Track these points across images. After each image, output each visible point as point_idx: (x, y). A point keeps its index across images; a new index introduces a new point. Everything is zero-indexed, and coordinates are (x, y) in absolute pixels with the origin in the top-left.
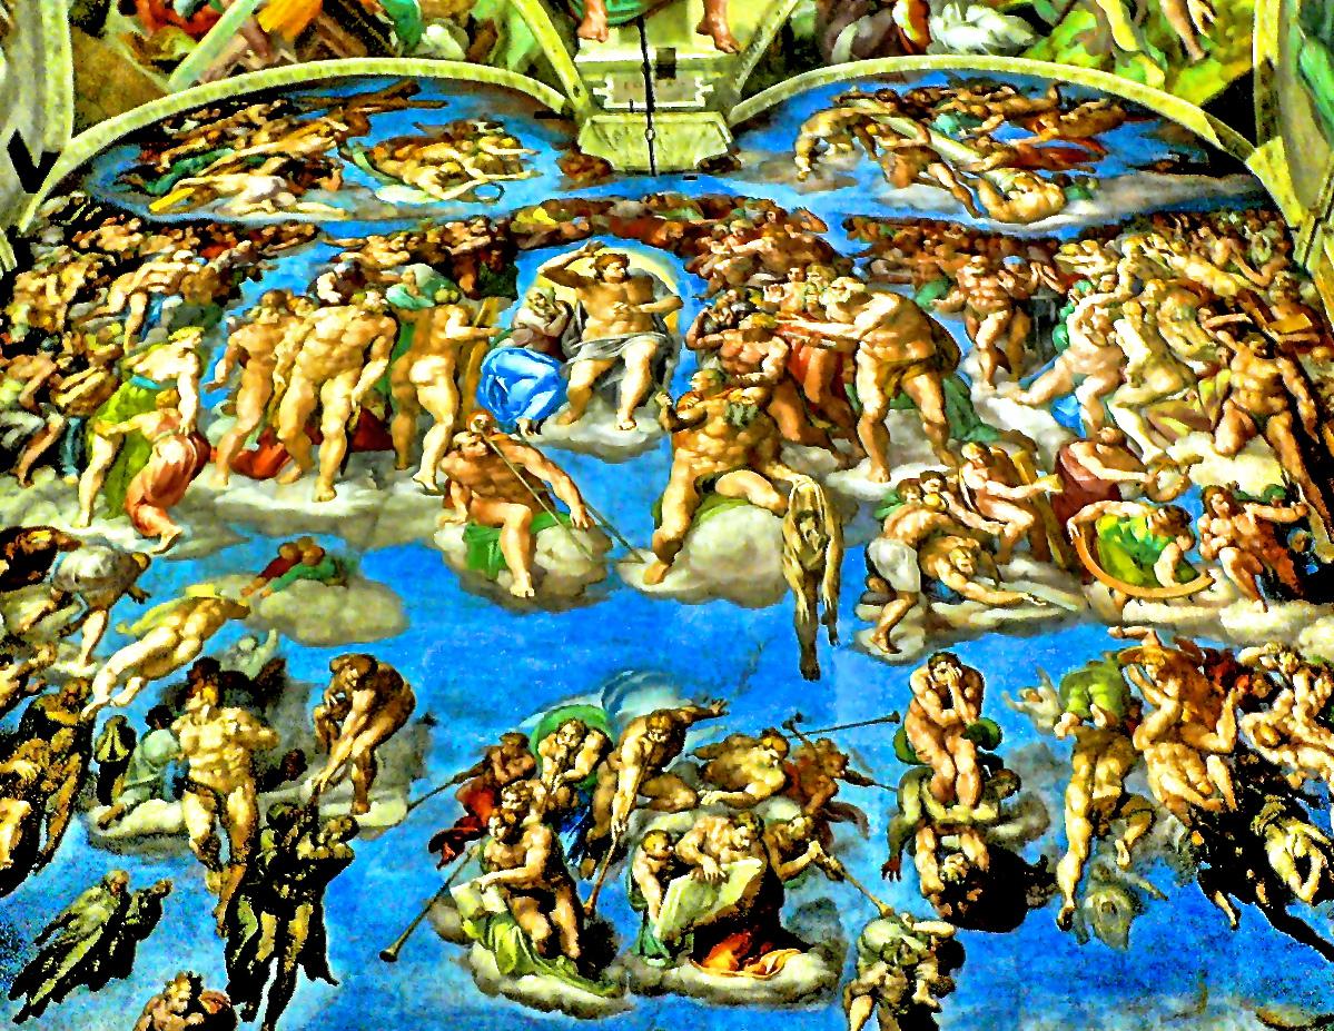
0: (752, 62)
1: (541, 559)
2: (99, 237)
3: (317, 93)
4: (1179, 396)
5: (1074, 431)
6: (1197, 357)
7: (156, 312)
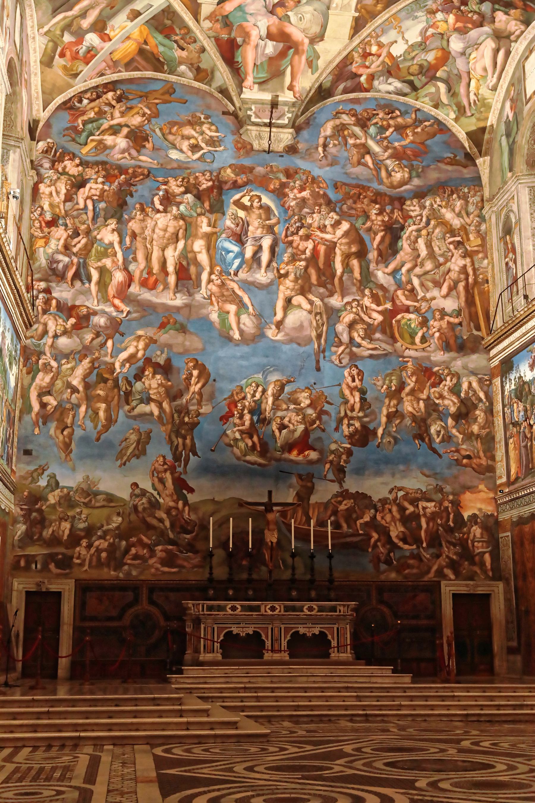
0: (306, 102)
1: (242, 326)
3: (133, 87)
4: (433, 273)
5: (399, 285)
6: (442, 255)
7: (98, 210)
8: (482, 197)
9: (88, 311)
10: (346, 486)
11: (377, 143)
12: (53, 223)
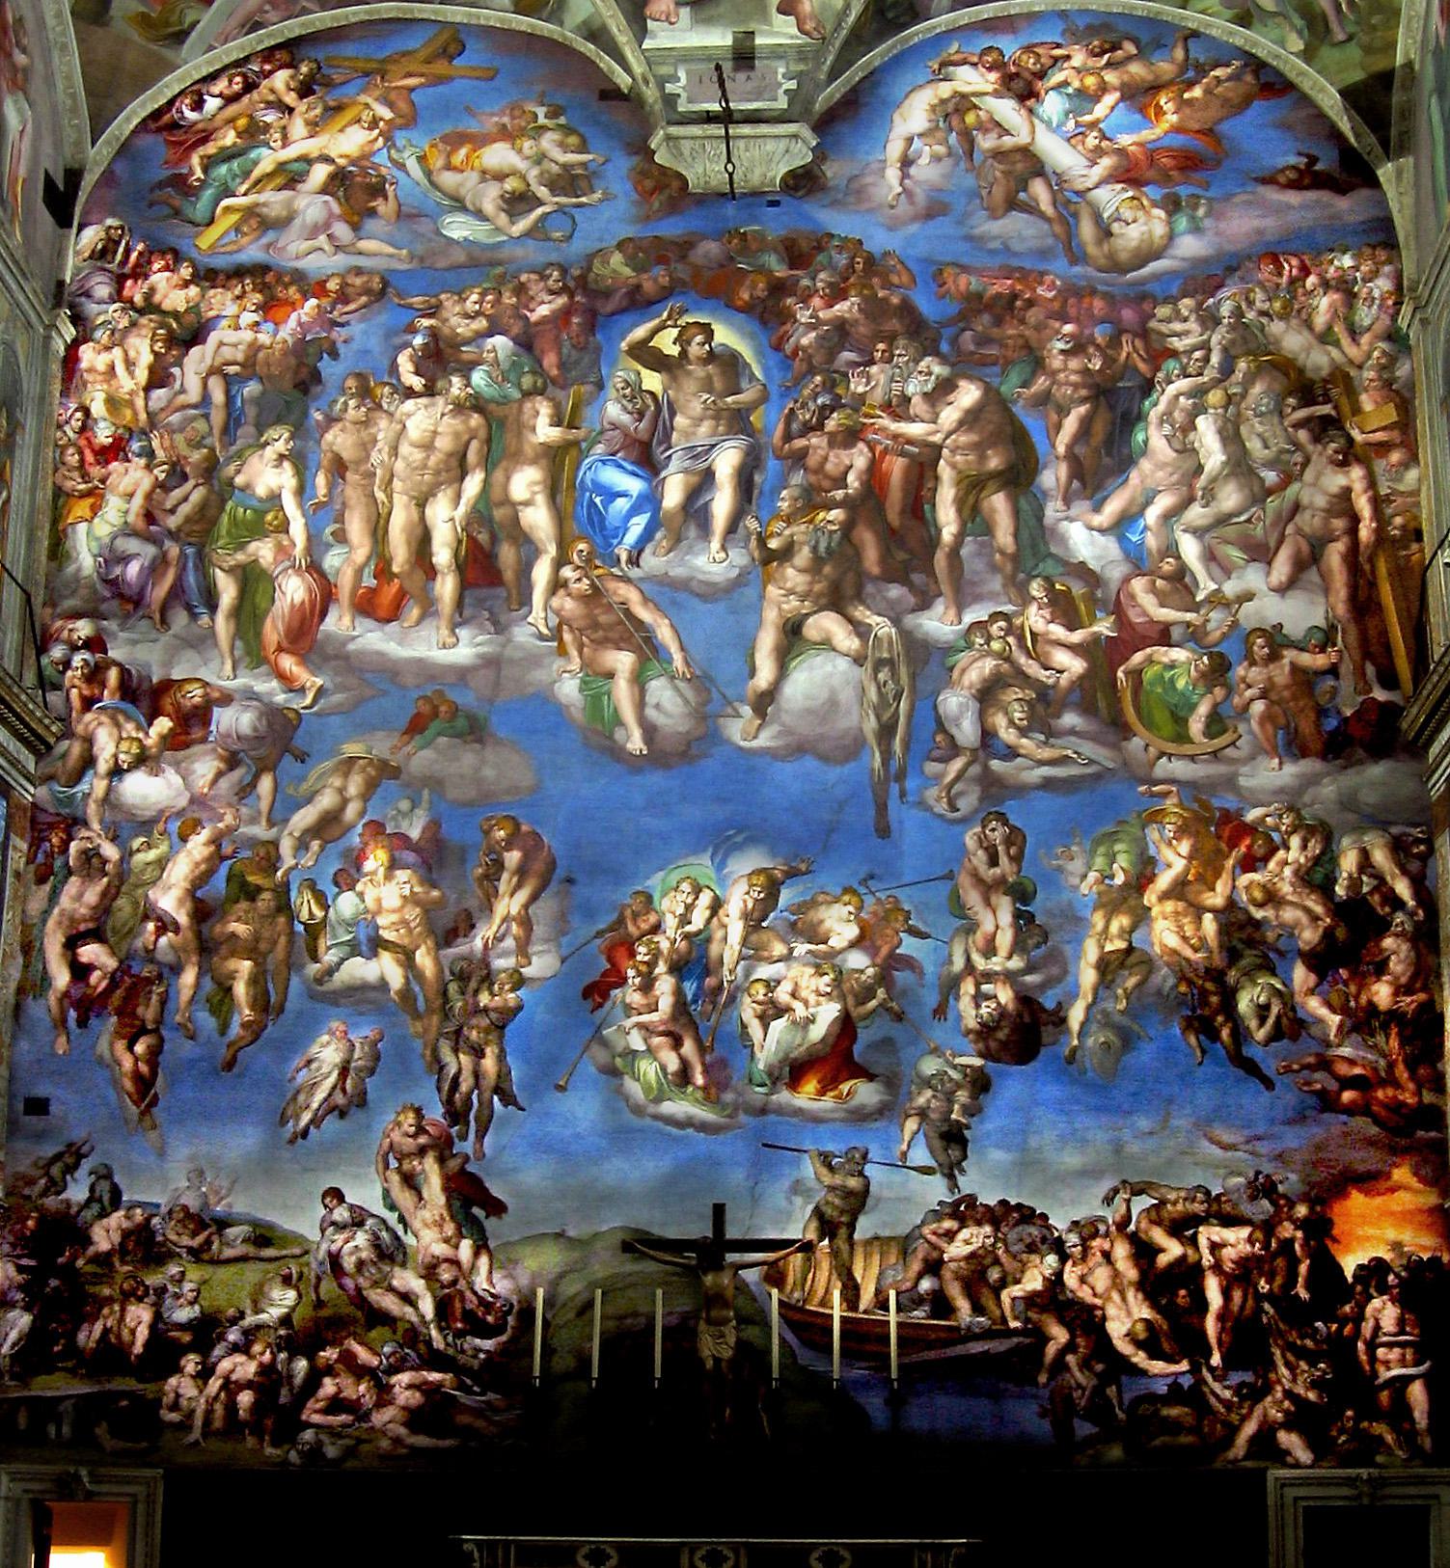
1: (651, 713)
2: (152, 290)
3: (349, 50)
4: (1242, 518)
5: (1138, 562)
6: (1270, 464)
9: (206, 695)
10: (967, 1184)
12: (115, 451)
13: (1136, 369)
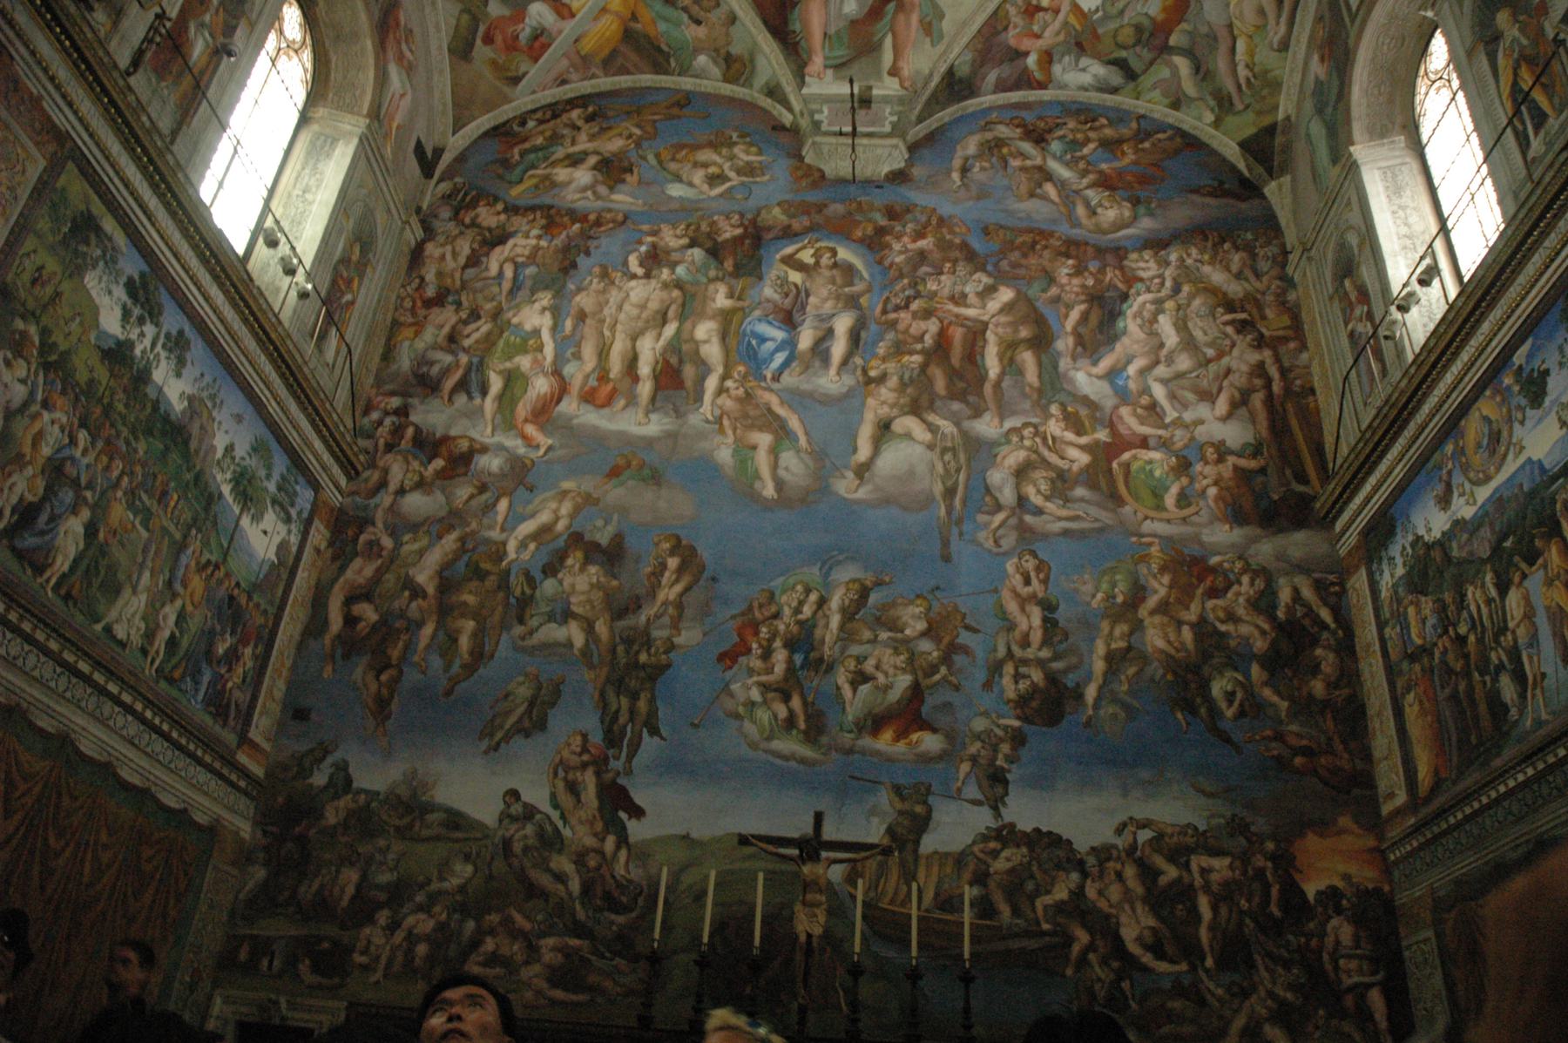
0: (924, 98)
1: (781, 473)
2: (477, 216)
5: (1123, 396)
6: (1210, 345)
8: (1283, 245)
9: (471, 447)
11: (1067, 164)
13: (1116, 287)
